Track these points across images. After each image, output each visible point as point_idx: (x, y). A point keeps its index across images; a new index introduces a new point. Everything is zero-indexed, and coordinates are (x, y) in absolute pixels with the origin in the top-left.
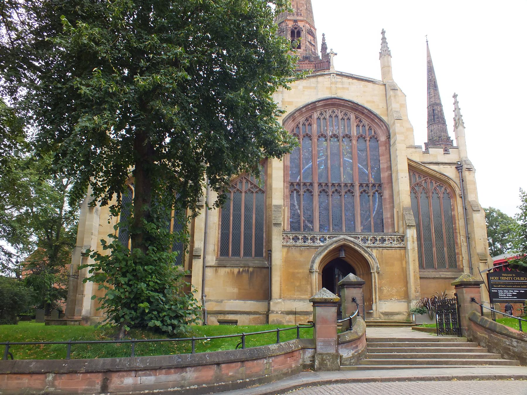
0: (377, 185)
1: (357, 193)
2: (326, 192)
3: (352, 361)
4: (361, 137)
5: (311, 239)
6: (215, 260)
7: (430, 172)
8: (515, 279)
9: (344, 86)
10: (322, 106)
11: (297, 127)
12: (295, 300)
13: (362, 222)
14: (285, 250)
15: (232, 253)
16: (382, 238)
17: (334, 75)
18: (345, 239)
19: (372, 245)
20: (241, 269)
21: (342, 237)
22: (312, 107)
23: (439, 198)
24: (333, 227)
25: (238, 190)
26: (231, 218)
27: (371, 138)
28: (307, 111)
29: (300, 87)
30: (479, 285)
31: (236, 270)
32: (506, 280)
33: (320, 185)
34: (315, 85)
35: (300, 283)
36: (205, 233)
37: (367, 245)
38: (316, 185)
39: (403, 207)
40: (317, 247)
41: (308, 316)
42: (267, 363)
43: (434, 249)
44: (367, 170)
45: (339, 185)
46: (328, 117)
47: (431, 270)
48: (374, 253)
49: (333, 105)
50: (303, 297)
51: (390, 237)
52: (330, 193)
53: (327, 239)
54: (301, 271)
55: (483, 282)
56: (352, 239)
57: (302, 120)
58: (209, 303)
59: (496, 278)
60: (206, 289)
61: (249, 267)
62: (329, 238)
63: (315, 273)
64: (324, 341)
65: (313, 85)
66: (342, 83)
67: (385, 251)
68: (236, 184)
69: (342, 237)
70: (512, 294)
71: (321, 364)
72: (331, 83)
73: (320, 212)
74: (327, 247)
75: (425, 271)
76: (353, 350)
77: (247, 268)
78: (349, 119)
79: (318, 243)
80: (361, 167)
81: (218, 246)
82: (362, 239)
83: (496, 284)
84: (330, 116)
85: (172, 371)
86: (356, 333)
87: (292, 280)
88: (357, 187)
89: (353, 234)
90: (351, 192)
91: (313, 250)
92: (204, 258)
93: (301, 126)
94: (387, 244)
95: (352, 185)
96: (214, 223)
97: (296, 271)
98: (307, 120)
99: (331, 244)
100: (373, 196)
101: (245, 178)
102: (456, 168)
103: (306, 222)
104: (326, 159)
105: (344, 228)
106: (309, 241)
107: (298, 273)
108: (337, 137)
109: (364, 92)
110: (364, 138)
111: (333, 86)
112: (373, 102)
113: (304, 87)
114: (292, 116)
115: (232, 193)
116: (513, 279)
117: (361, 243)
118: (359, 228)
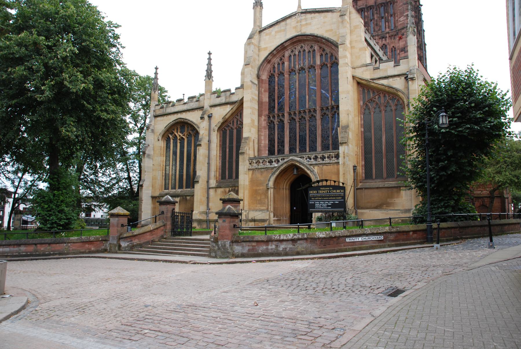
0: (335, 107)
1: (318, 116)
2: (295, 120)
3: (127, 249)
4: (323, 66)
5: (269, 162)
6: (215, 182)
7: (380, 86)
8: (332, 191)
9: (307, 22)
10: (291, 44)
11: (274, 67)
12: (256, 210)
13: (322, 142)
14: (251, 172)
15: (228, 176)
16: (323, 156)
17: (300, 14)
18: (292, 160)
19: (314, 162)
20: (231, 189)
21: (291, 158)
22: (282, 48)
23: (391, 110)
24: (300, 149)
25: (232, 128)
26: (227, 150)
27: (332, 64)
28: (278, 52)
29: (273, 33)
30: (175, 204)
31: (227, 189)
32: (324, 193)
33: (290, 114)
34: (284, 28)
35: (261, 197)
36: (209, 164)
37: (310, 163)
38: (286, 115)
39: (342, 126)
40: (273, 168)
41: (264, 223)
42: (66, 246)
43: (384, 161)
44: (328, 94)
45: (305, 112)
46: (297, 53)
47: (379, 180)
48: (316, 169)
49: (300, 41)
50: (262, 208)
51: (330, 155)
52: (297, 120)
53: (280, 161)
54: (261, 188)
55: (177, 202)
56: (298, 159)
57: (276, 60)
58: (211, 214)
59: (314, 192)
60: (210, 204)
61: (235, 187)
62: (281, 160)
63: (270, 189)
64: (112, 237)
65: (283, 28)
66: (306, 19)
67: (325, 167)
68: (230, 123)
69: (291, 158)
70: (327, 205)
71: (110, 249)
72: (297, 22)
73: (290, 138)
74: (279, 167)
75: (373, 181)
76: (128, 242)
77: (234, 188)
78: (314, 50)
79: (275, 165)
80: (324, 92)
81: (219, 172)
82: (306, 159)
83: (313, 197)
84: (300, 52)
85: (16, 246)
86: (133, 233)
87: (255, 196)
88: (318, 112)
89: (300, 154)
90: (313, 117)
91: (270, 171)
92: (208, 182)
93: (276, 66)
94: (327, 160)
95: (315, 111)
96: (214, 156)
97: (258, 188)
98: (281, 59)
99: (282, 165)
100: (332, 117)
101: (236, 118)
102: (405, 78)
103: (280, 146)
104: (295, 91)
105: (308, 149)
106: (268, 164)
107: (259, 190)
108: (304, 69)
109: (324, 23)
110: (327, 65)
111: (299, 24)
112: (331, 30)
113: (276, 32)
114: (267, 60)
115: (228, 132)
116: (330, 192)
117: (305, 161)
118: (319, 148)
